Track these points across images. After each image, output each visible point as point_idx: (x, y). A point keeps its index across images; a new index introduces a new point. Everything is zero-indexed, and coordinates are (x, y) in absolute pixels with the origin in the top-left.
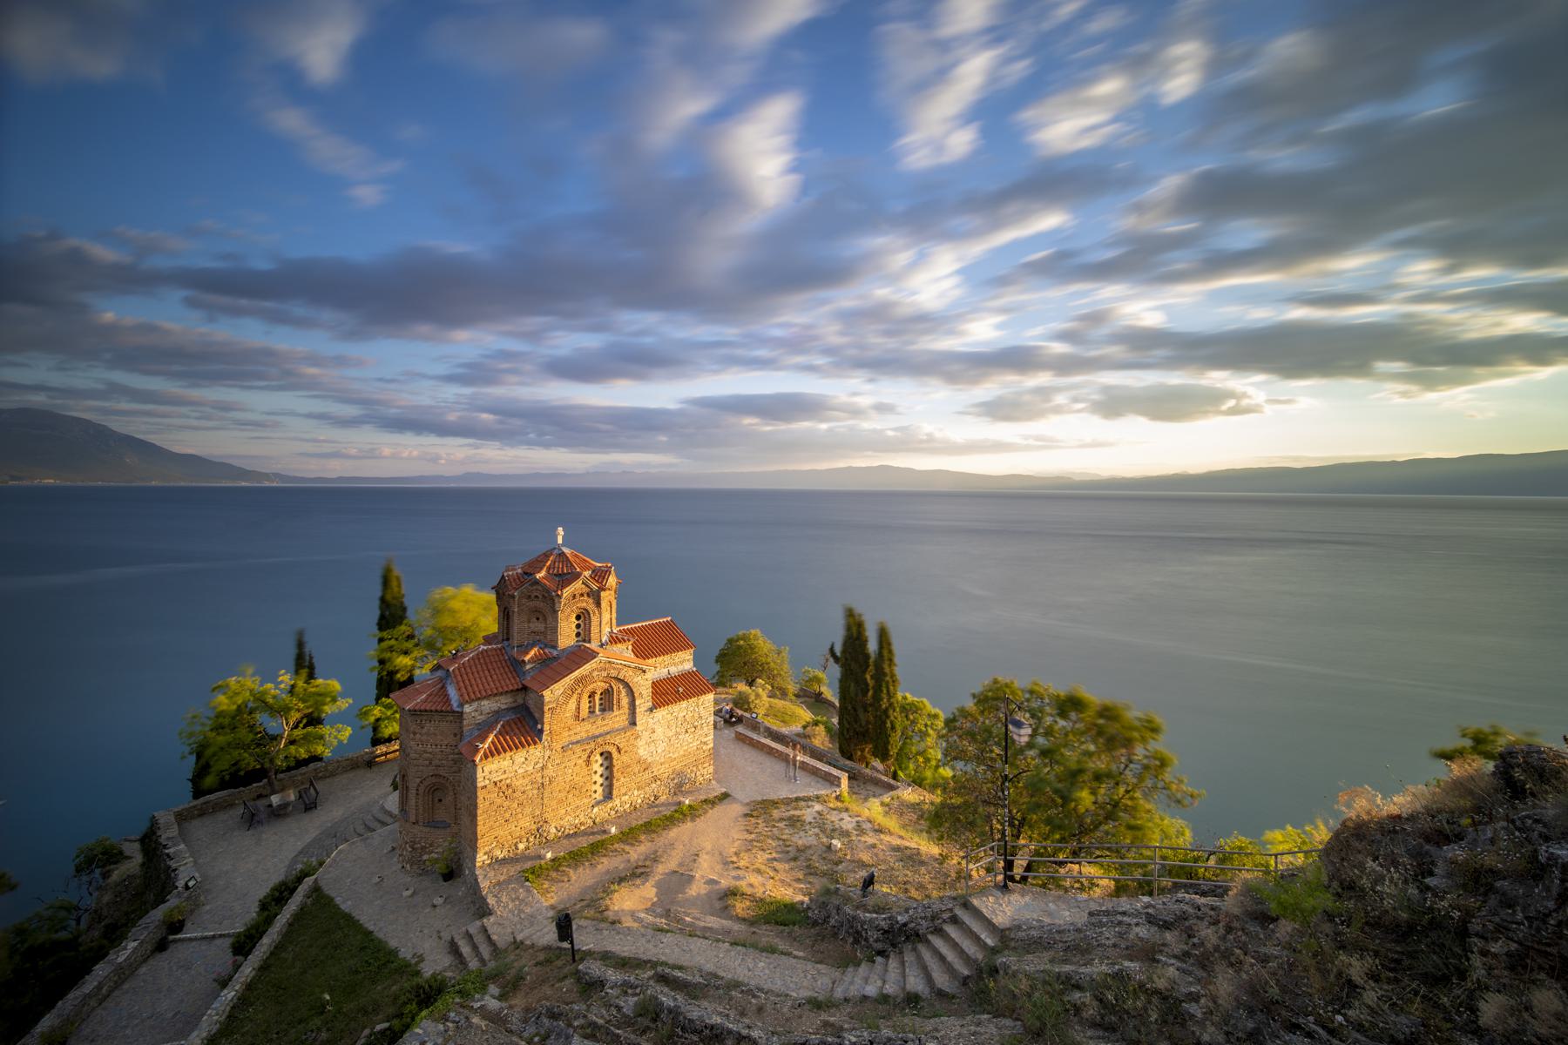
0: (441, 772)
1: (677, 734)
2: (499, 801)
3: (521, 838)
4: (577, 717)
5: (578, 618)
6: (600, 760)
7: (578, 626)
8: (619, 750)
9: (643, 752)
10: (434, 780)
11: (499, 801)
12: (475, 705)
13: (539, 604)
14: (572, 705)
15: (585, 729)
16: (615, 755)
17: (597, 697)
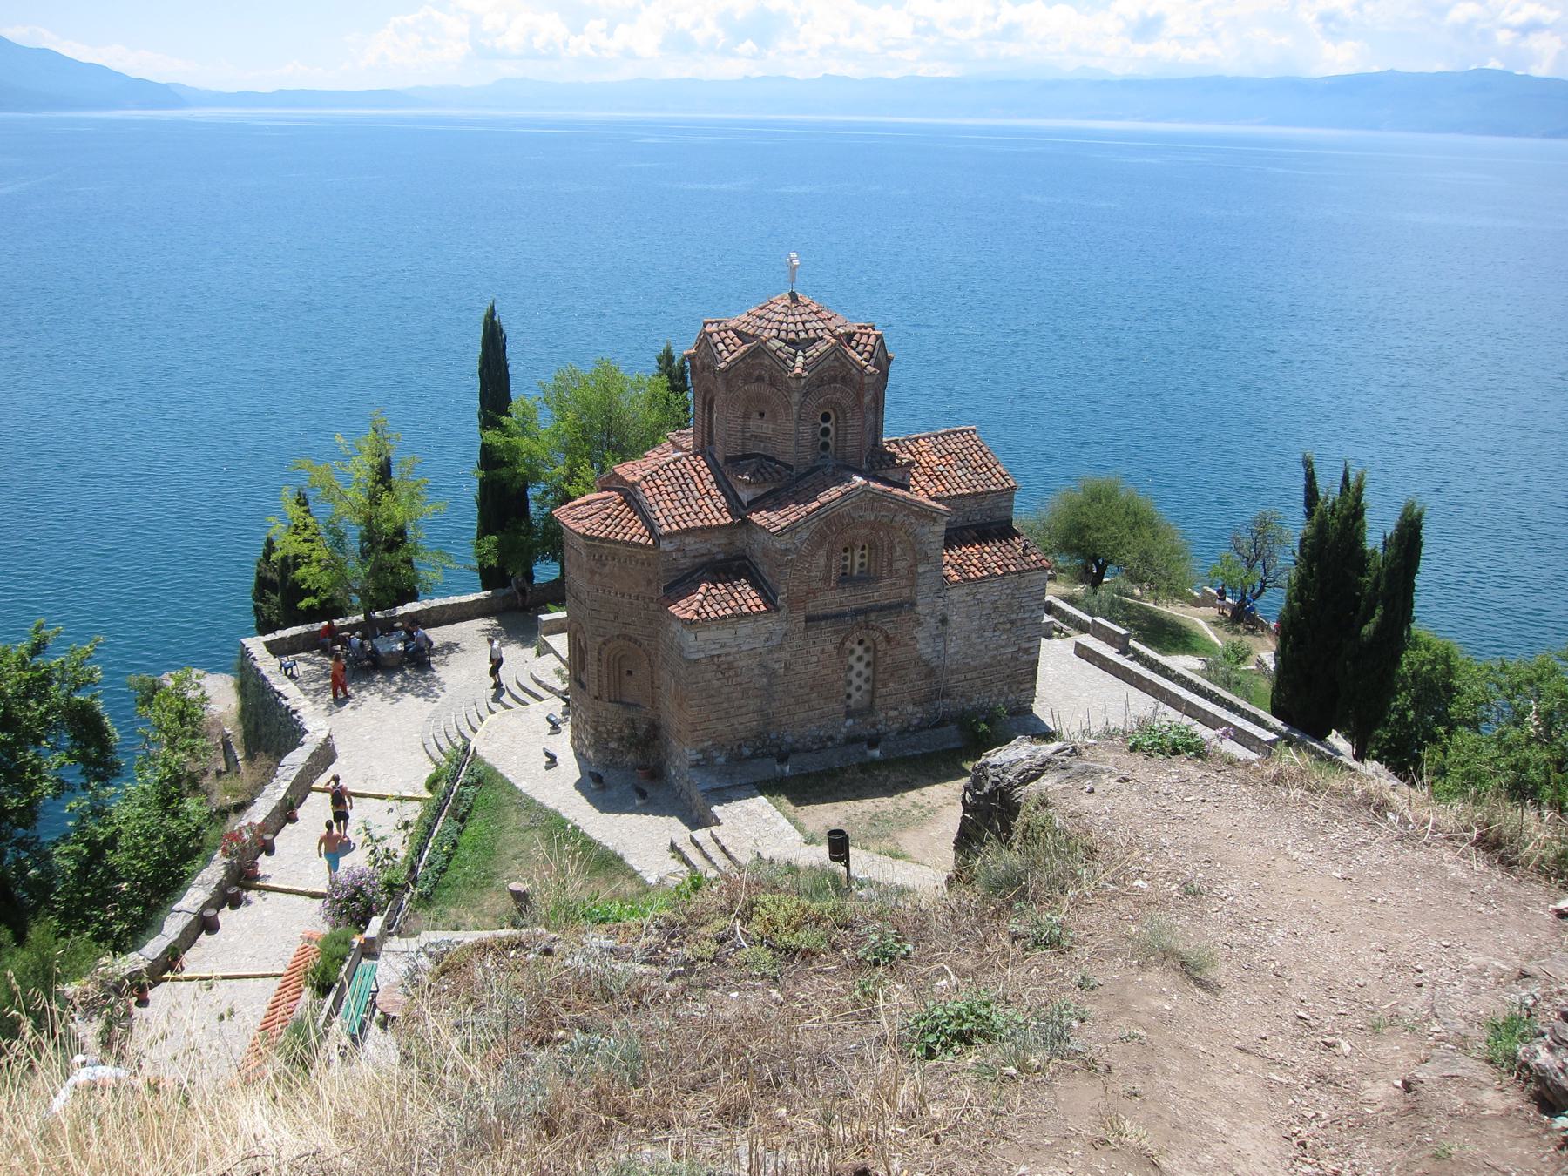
0: (631, 631)
1: (982, 629)
2: (716, 684)
3: (746, 739)
4: (827, 579)
5: (826, 418)
6: (859, 650)
7: (825, 432)
8: (888, 639)
9: (924, 648)
10: (621, 642)
11: (716, 684)
12: (677, 541)
13: (764, 389)
14: (822, 562)
15: (835, 599)
16: (882, 646)
17: (857, 553)
